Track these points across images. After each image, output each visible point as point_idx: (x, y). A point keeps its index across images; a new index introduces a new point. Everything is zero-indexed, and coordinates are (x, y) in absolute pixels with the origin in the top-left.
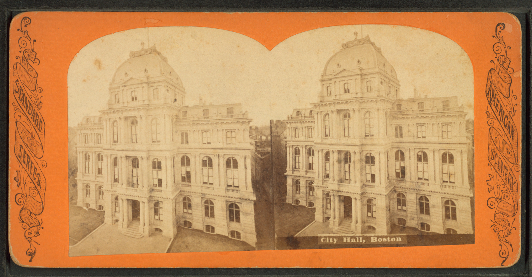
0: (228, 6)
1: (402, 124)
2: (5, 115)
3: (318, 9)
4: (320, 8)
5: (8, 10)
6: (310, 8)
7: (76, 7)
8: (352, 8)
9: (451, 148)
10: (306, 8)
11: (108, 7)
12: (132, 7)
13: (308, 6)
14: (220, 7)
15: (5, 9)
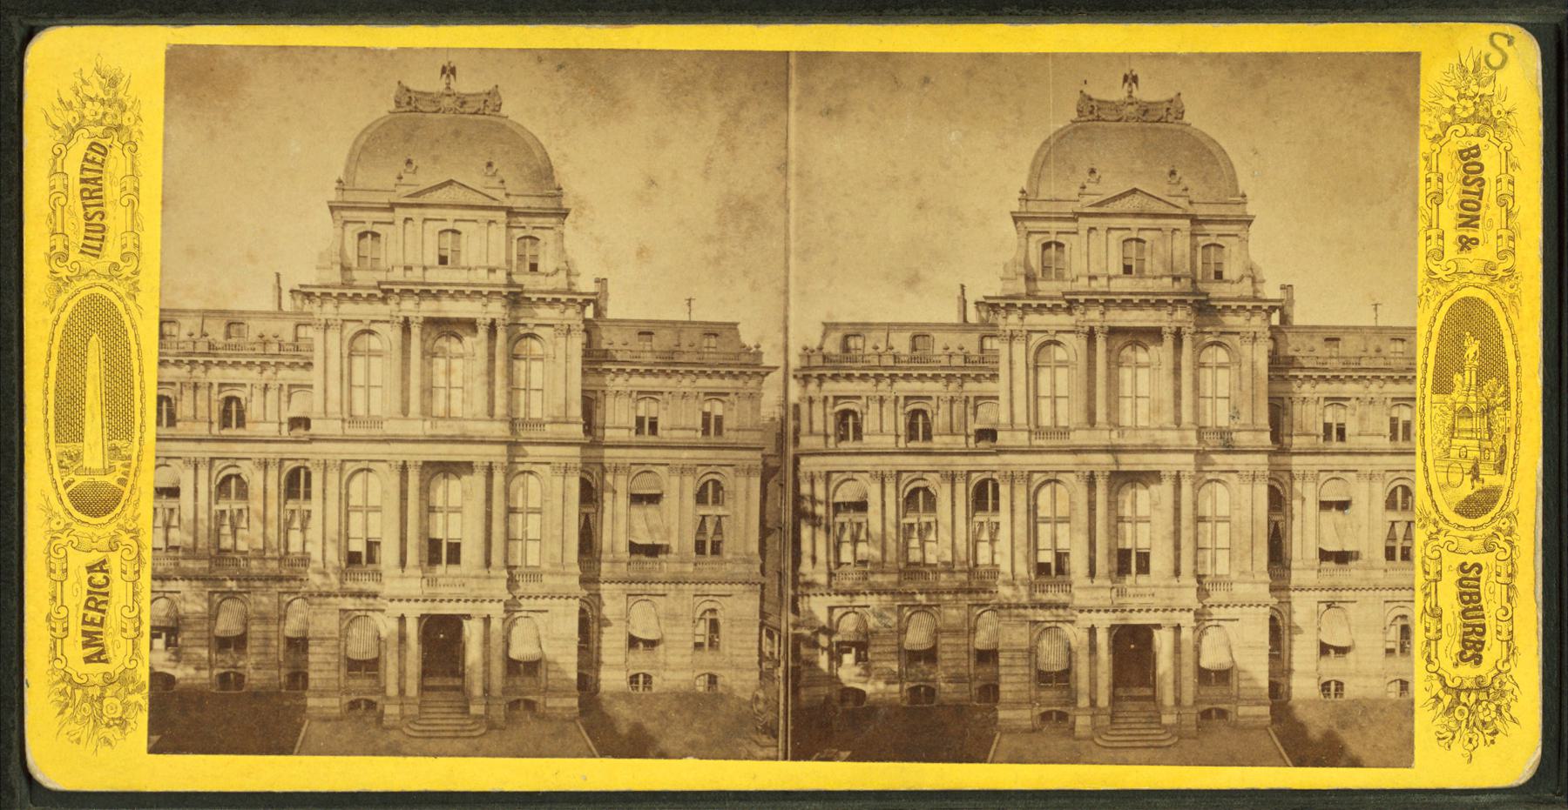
0: (675, 9)
1: (595, 392)
2: (15, 333)
3: (941, 14)
4: (945, 11)
5: (21, 24)
6: (916, 11)
7: (223, 12)
8: (1041, 11)
9: (1062, 468)
10: (905, 11)
11: (316, 12)
12: (389, 10)
13: (910, 6)
14: (648, 12)
15: (14, 19)
